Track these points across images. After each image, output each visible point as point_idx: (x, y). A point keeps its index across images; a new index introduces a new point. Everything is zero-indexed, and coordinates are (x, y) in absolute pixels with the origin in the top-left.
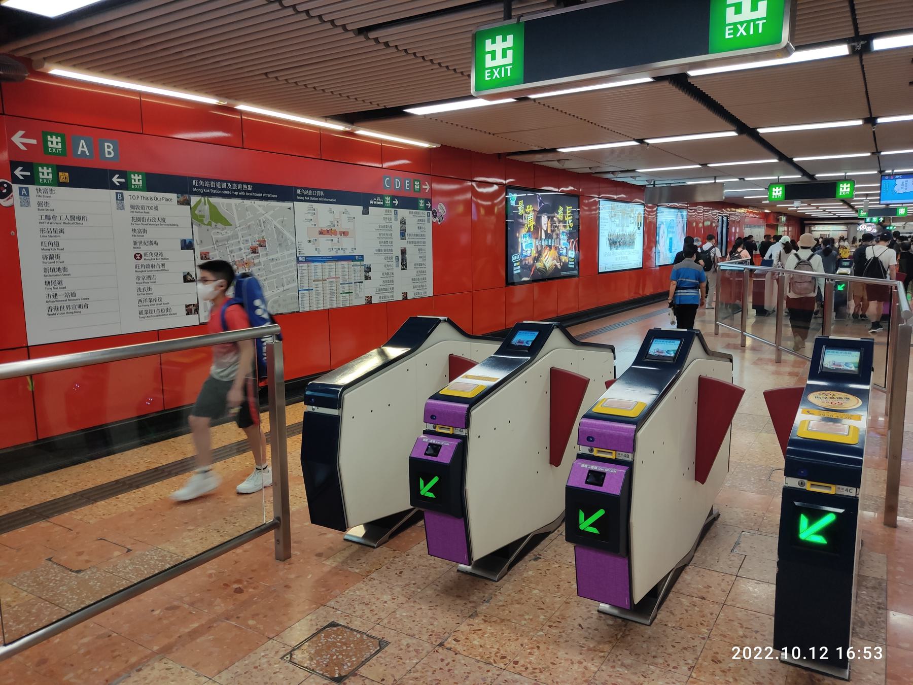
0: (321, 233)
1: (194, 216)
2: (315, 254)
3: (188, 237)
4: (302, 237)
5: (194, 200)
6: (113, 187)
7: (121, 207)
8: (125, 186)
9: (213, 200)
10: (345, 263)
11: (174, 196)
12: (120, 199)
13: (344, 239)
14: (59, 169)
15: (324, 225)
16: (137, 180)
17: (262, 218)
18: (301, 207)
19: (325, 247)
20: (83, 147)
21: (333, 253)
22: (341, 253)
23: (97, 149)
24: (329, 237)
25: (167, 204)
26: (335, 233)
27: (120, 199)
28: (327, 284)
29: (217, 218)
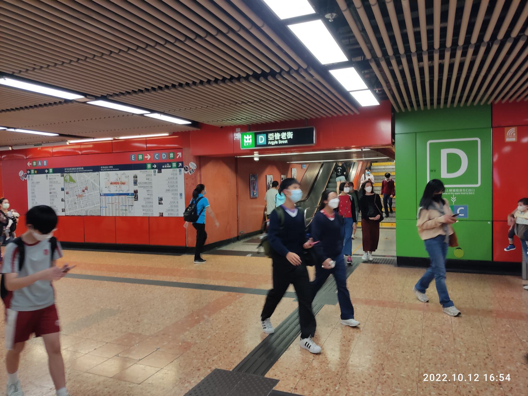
0: (111, 184)
1: (65, 180)
2: (109, 192)
3: (63, 187)
4: (103, 185)
5: (65, 174)
6: (46, 173)
7: (47, 179)
8: (48, 173)
9: (71, 174)
10: (124, 197)
11: (60, 174)
12: (47, 176)
13: (123, 186)
14: (35, 170)
15: (113, 180)
16: (51, 170)
17: (87, 179)
18: (102, 174)
19: (113, 189)
20: (40, 164)
21: (117, 192)
22: (121, 192)
23: (42, 163)
24: (115, 185)
25: (58, 176)
26: (118, 183)
27: (47, 176)
28: (114, 205)
29: (72, 180)
